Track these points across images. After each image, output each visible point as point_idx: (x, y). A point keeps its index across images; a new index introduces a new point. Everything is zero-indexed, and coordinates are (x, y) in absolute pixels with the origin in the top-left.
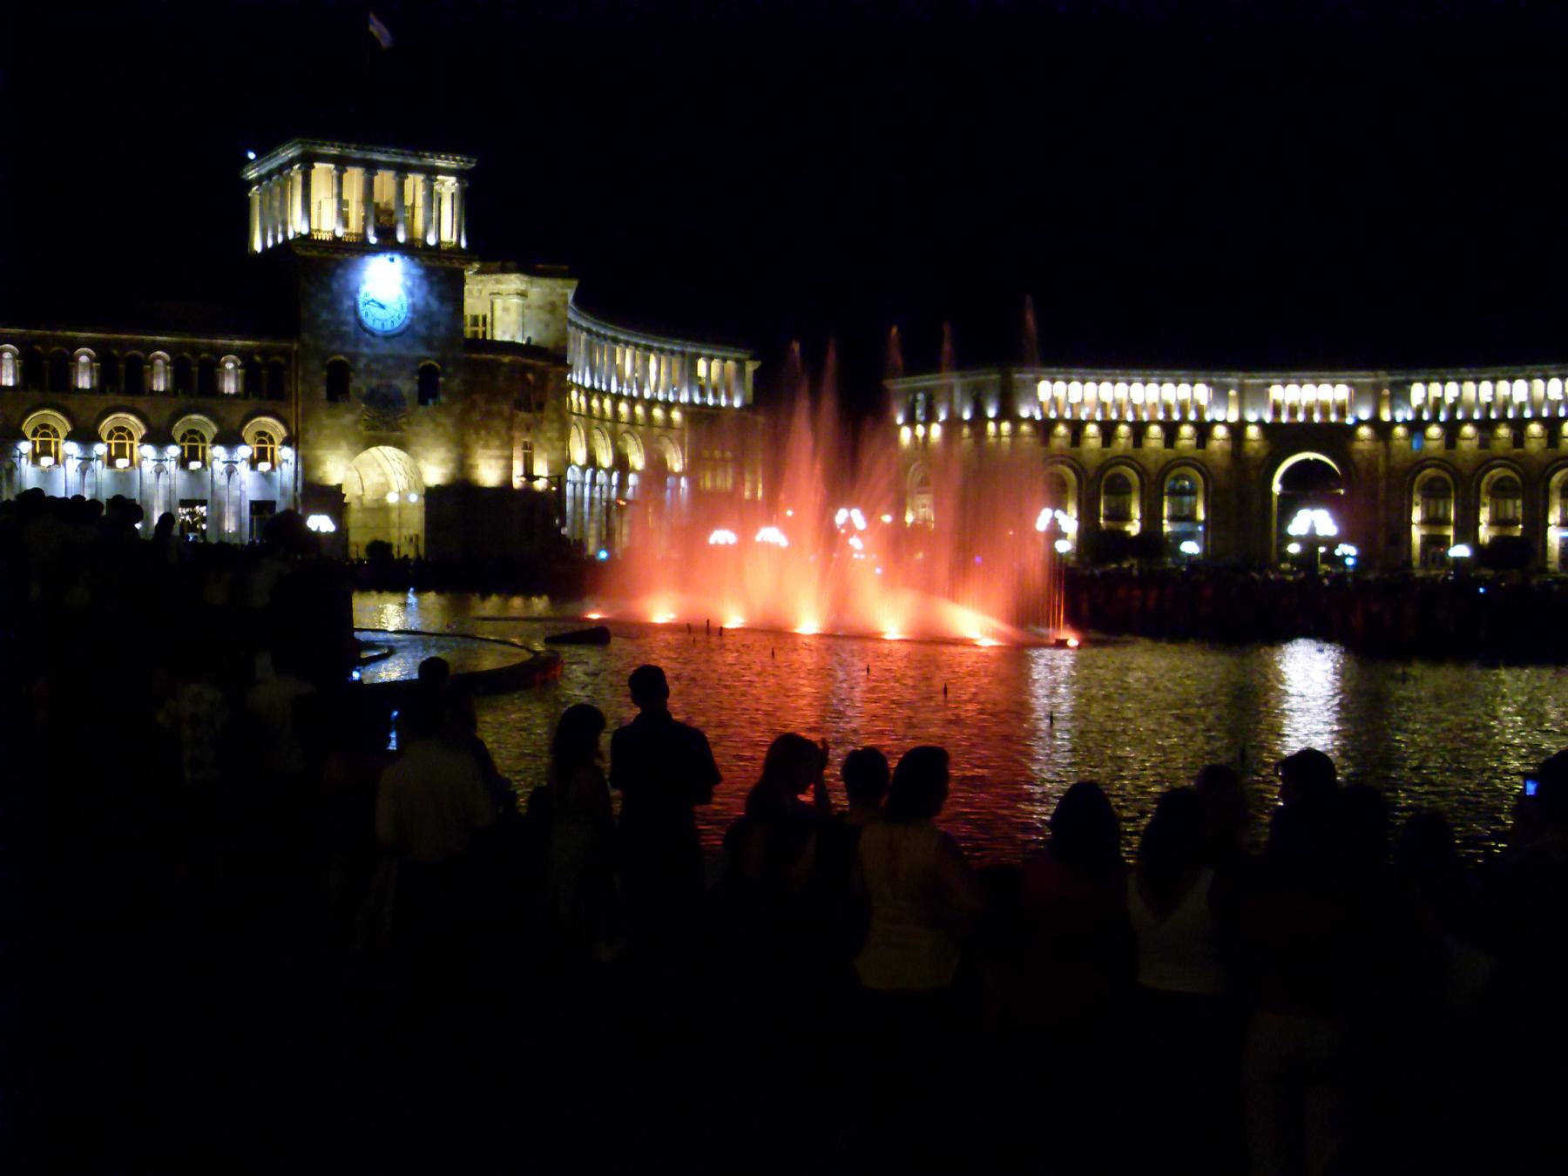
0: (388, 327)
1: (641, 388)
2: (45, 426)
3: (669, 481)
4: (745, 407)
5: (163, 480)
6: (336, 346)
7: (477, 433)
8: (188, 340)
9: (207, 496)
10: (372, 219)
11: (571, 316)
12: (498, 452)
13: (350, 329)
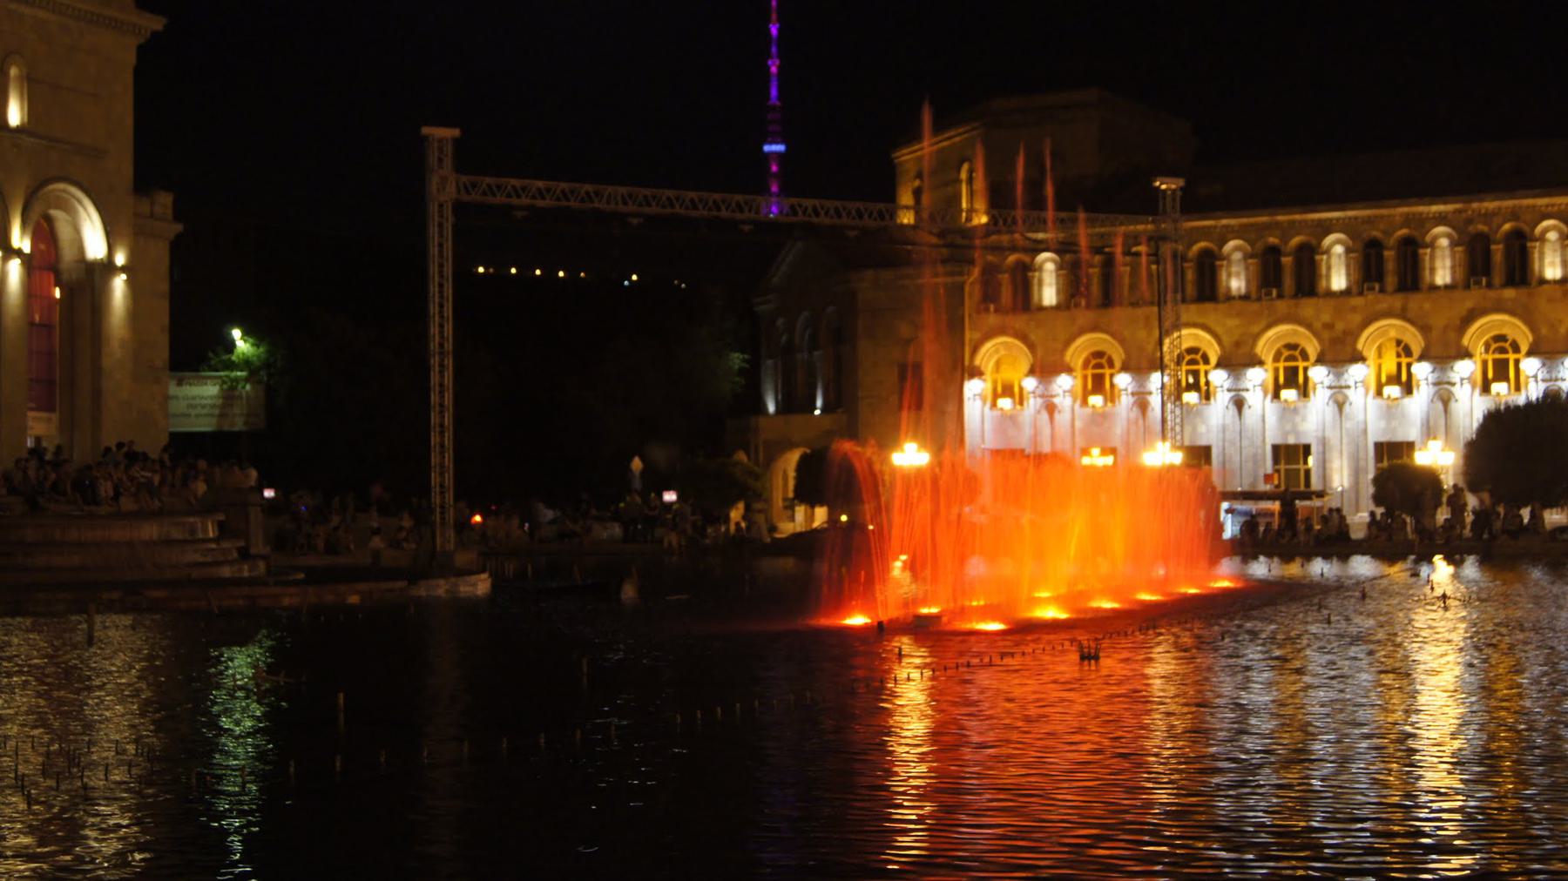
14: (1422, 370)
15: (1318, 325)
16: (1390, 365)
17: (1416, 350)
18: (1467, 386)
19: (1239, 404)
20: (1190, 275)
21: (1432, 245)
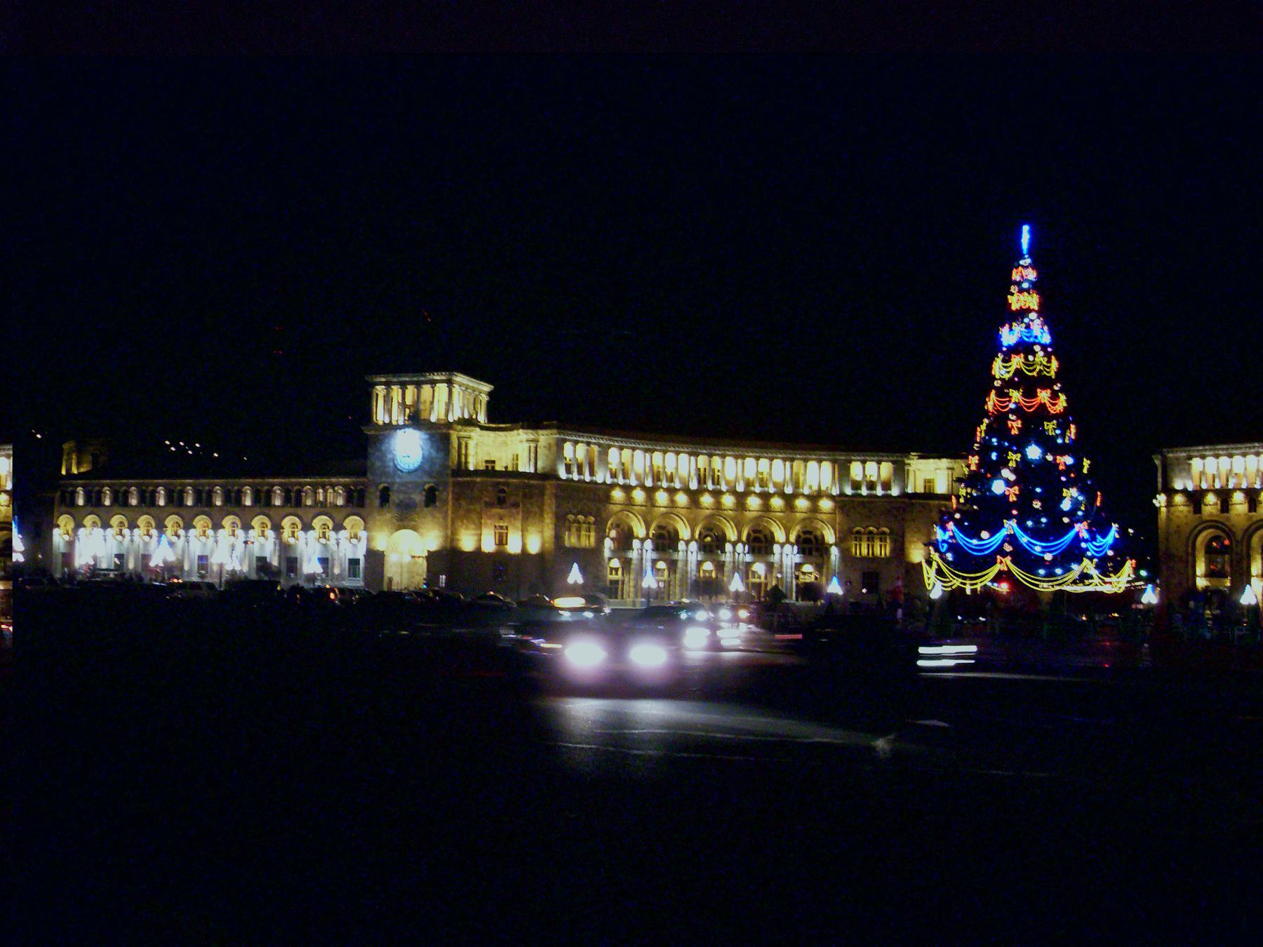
0: (412, 467)
13: (391, 470)
19: (132, 541)
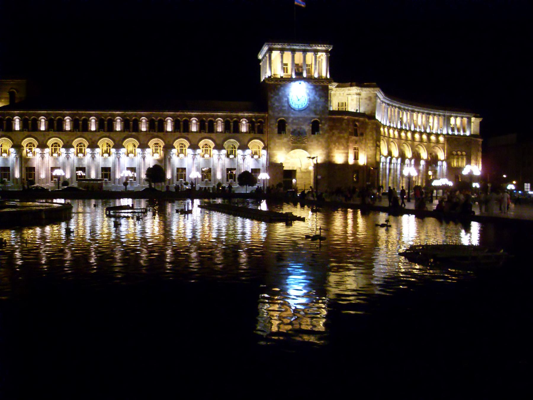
0: (300, 107)
1: (425, 129)
2: (182, 144)
3: (439, 163)
4: (471, 135)
5: (221, 162)
6: (281, 115)
7: (335, 144)
8: (229, 114)
9: (236, 167)
10: (294, 70)
11: (387, 102)
12: (342, 151)
13: (286, 108)
14: (113, 151)
15: (88, 139)
16: (105, 148)
17: (112, 146)
18: (124, 155)
19: (68, 157)
20: (55, 125)
21: (116, 121)
